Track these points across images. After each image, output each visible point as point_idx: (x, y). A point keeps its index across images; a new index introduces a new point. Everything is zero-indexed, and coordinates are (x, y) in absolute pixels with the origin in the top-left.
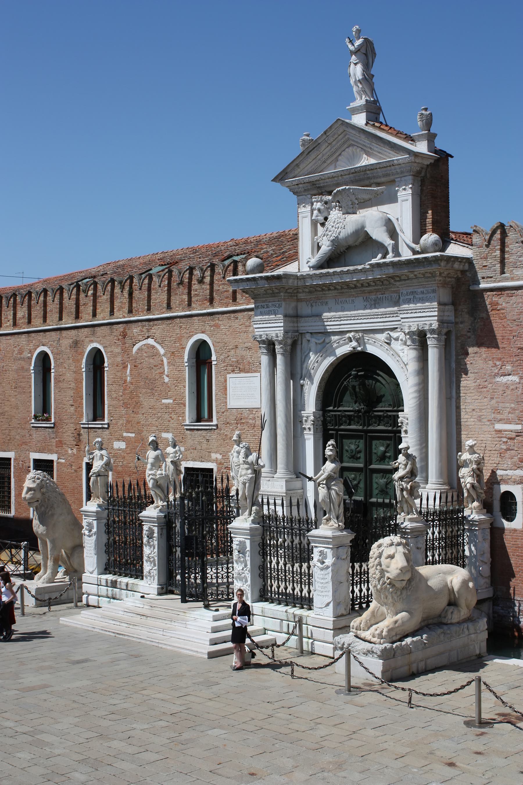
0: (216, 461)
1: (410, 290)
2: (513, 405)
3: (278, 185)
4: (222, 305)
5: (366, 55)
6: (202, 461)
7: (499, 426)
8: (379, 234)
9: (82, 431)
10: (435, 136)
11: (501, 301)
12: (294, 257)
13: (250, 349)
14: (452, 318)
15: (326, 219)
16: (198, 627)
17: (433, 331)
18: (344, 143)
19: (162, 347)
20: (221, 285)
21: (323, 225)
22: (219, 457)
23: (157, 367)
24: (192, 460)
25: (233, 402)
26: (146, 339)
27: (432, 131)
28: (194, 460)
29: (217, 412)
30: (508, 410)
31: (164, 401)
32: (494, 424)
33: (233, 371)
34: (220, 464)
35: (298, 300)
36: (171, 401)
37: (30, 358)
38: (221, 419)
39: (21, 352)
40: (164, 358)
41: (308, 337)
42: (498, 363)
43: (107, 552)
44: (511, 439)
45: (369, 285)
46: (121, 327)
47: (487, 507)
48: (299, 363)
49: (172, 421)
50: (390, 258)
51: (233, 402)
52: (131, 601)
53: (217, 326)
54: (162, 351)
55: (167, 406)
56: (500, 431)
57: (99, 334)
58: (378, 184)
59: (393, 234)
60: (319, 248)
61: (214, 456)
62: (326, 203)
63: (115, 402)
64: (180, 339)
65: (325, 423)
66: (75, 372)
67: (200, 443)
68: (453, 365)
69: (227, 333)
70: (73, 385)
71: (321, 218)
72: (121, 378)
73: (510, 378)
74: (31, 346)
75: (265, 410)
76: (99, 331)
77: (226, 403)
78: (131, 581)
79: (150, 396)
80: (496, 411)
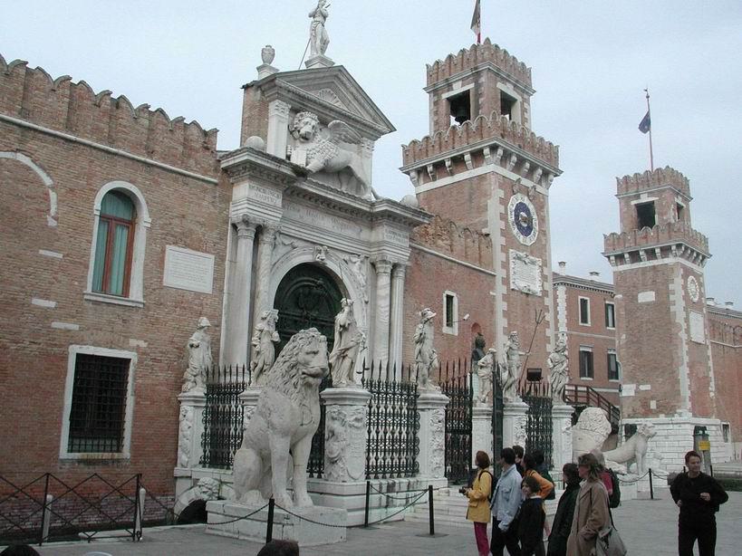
0: (138, 349)
1: (391, 229)
4: (164, 160)
6: (111, 348)
13: (203, 225)
17: (406, 267)
19: (48, 175)
20: (167, 137)
22: (143, 344)
23: (34, 201)
24: (93, 345)
26: (12, 151)
28: (96, 344)
31: (42, 252)
33: (175, 243)
34: (144, 354)
36: (61, 256)
38: (152, 297)
40: (50, 191)
49: (58, 285)
54: (48, 181)
55: (50, 261)
61: (133, 342)
64: (90, 176)
67: (110, 322)
69: (171, 197)
75: (130, 298)
77: (161, 278)
79: (11, 237)
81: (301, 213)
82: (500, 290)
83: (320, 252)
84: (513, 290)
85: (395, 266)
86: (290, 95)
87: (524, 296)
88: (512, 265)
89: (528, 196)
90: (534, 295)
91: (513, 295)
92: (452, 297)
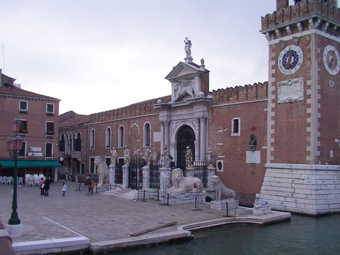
1: (196, 107)
2: (221, 138)
3: (166, 80)
5: (189, 44)
7: (218, 144)
8: (190, 92)
9: (118, 149)
10: (205, 66)
11: (218, 110)
12: (171, 100)
14: (207, 115)
15: (177, 89)
16: (133, 194)
18: (182, 68)
21: (177, 90)
25: (155, 140)
27: (204, 64)
29: (151, 143)
30: (220, 139)
31: (138, 140)
32: (216, 143)
33: (155, 132)
35: (171, 111)
36: (140, 140)
37: (106, 130)
39: (103, 128)
41: (173, 121)
42: (218, 127)
43: (115, 178)
44: (221, 147)
45: (187, 106)
46: (128, 120)
47: (215, 166)
48: (171, 129)
50: (193, 98)
51: (155, 140)
52: (118, 189)
53: (151, 119)
54: (138, 126)
55: (139, 141)
56: (218, 145)
57: (123, 122)
58: (191, 79)
59: (193, 93)
60: (176, 96)
62: (177, 84)
63: (126, 141)
65: (178, 145)
66: (117, 133)
68: (207, 128)
70: (116, 137)
71: (176, 89)
72: (128, 134)
73: (221, 130)
74: (106, 127)
76: (123, 122)
78: (120, 185)
80: (217, 140)
81: (179, 112)
82: (271, 105)
83: (183, 121)
84: (279, 103)
85: (199, 119)
86: (172, 80)
87: (289, 104)
88: (279, 91)
89: (295, 44)
90: (296, 101)
91: (279, 106)
92: (238, 120)
